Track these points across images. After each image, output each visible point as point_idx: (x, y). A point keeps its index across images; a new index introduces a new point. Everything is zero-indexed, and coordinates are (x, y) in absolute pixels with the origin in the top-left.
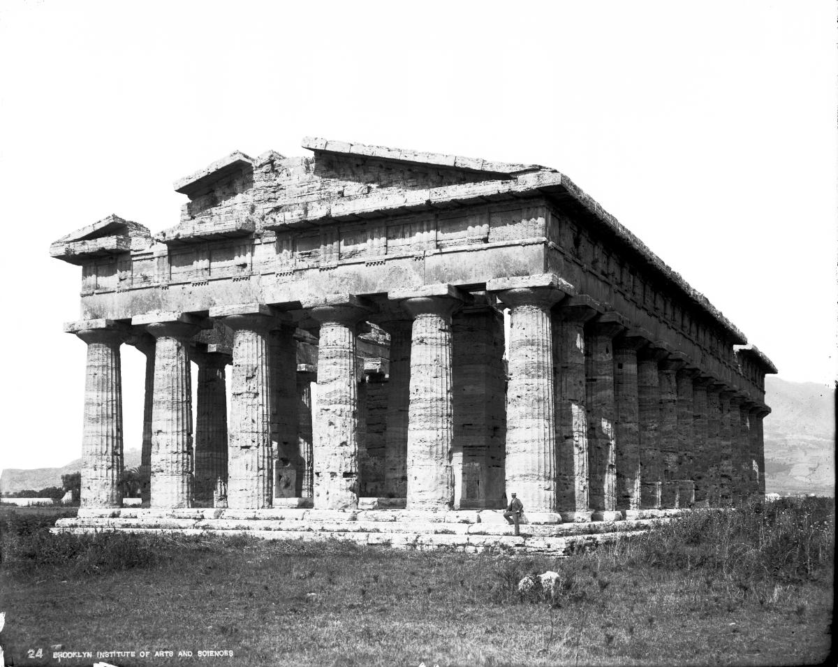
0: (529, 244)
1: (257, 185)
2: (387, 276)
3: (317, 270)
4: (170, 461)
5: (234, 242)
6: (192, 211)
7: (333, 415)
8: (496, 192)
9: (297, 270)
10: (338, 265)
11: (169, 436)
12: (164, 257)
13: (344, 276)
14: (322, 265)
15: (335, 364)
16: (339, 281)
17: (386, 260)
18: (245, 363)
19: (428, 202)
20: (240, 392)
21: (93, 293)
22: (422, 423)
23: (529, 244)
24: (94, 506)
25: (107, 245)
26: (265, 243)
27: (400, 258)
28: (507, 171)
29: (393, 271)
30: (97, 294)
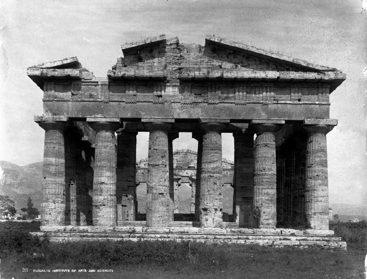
0: (323, 105)
1: (168, 54)
2: (247, 111)
3: (206, 104)
4: (109, 200)
5: (154, 83)
6: (124, 63)
7: (216, 179)
8: (314, 78)
9: (194, 103)
11: (109, 186)
12: (106, 85)
13: (222, 108)
14: (210, 101)
15: (216, 153)
16: (219, 111)
17: (247, 103)
18: (160, 149)
19: (278, 78)
20: (157, 164)
21: (53, 100)
22: (267, 186)
23: (323, 105)
24: (54, 225)
25: (73, 73)
26: (172, 86)
27: (255, 103)
28: (320, 69)
30: (55, 101)
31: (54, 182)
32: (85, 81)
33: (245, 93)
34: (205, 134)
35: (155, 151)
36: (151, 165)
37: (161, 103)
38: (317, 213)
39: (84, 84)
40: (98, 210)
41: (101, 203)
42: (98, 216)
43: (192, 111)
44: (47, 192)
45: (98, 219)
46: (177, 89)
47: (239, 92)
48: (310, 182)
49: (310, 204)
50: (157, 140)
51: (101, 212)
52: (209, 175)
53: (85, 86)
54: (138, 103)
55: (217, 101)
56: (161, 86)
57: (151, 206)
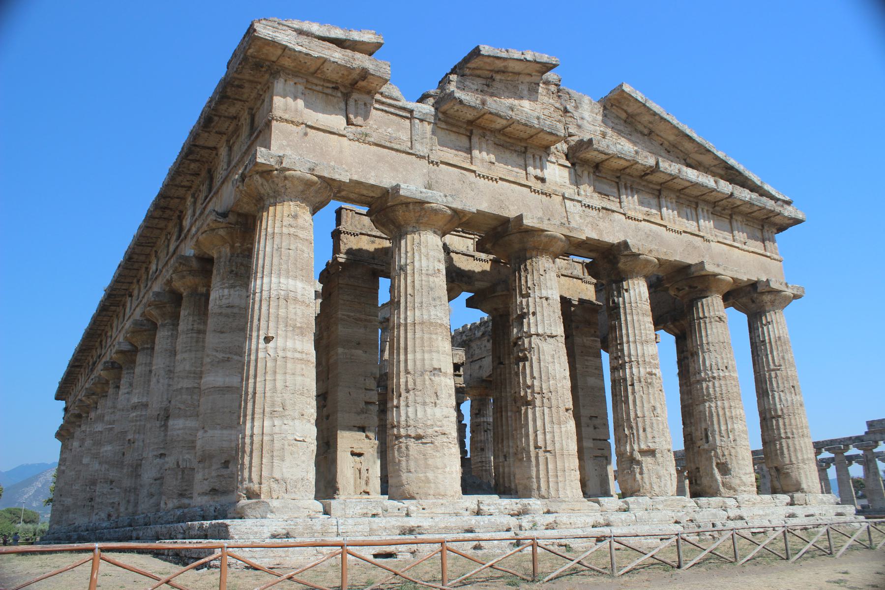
10: (645, 220)
13: (648, 232)
14: (630, 213)
20: (554, 334)
29: (690, 244)
31: (298, 355)
32: (384, 100)
33: (676, 212)
34: (625, 279)
35: (544, 300)
36: (538, 335)
37: (546, 194)
38: (808, 459)
39: (377, 106)
40: (429, 448)
41: (437, 429)
42: (427, 466)
43: (602, 225)
44: (279, 385)
45: (430, 475)
46: (565, 173)
47: (668, 209)
48: (783, 398)
49: (790, 441)
50: (547, 275)
51: (438, 454)
52: (648, 370)
53: (379, 112)
54: (500, 182)
55: (641, 217)
56: (540, 158)
57: (549, 442)
